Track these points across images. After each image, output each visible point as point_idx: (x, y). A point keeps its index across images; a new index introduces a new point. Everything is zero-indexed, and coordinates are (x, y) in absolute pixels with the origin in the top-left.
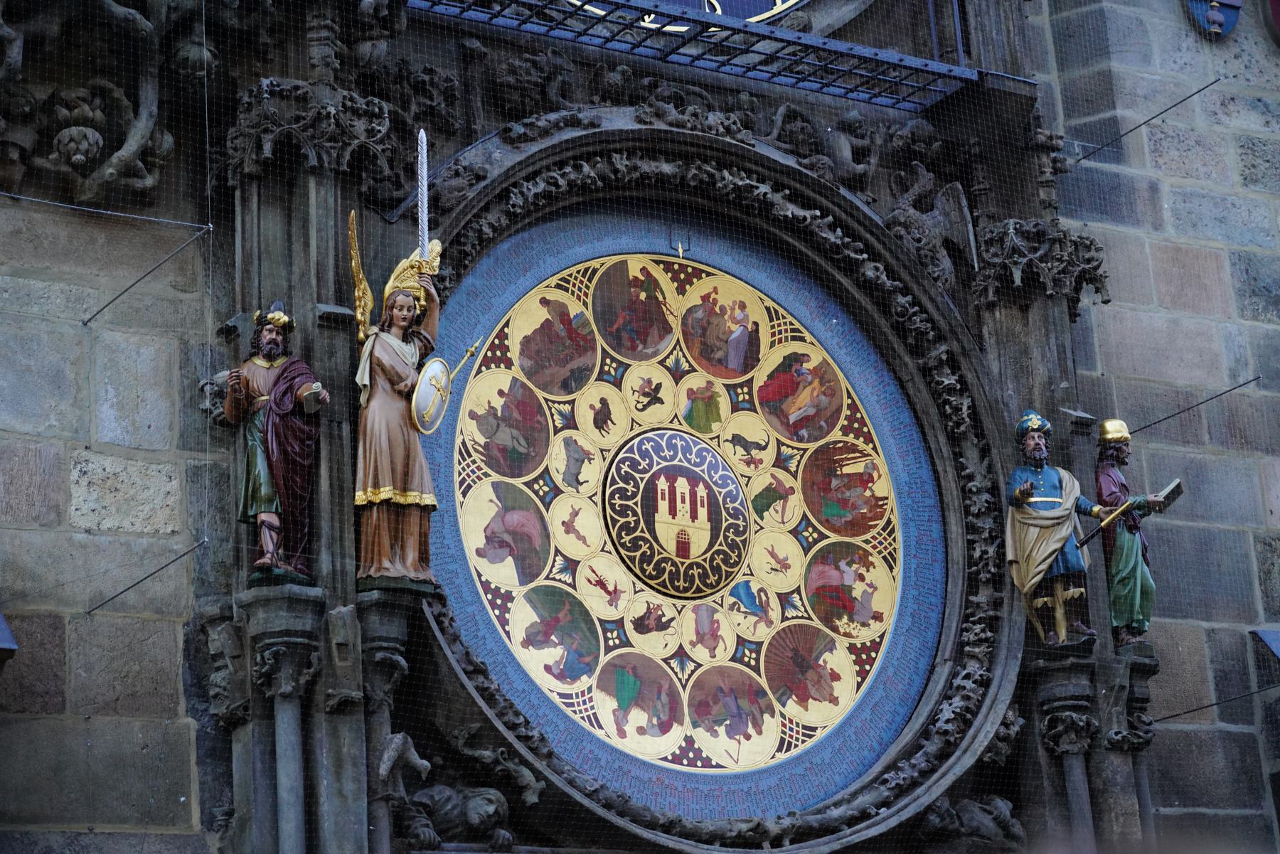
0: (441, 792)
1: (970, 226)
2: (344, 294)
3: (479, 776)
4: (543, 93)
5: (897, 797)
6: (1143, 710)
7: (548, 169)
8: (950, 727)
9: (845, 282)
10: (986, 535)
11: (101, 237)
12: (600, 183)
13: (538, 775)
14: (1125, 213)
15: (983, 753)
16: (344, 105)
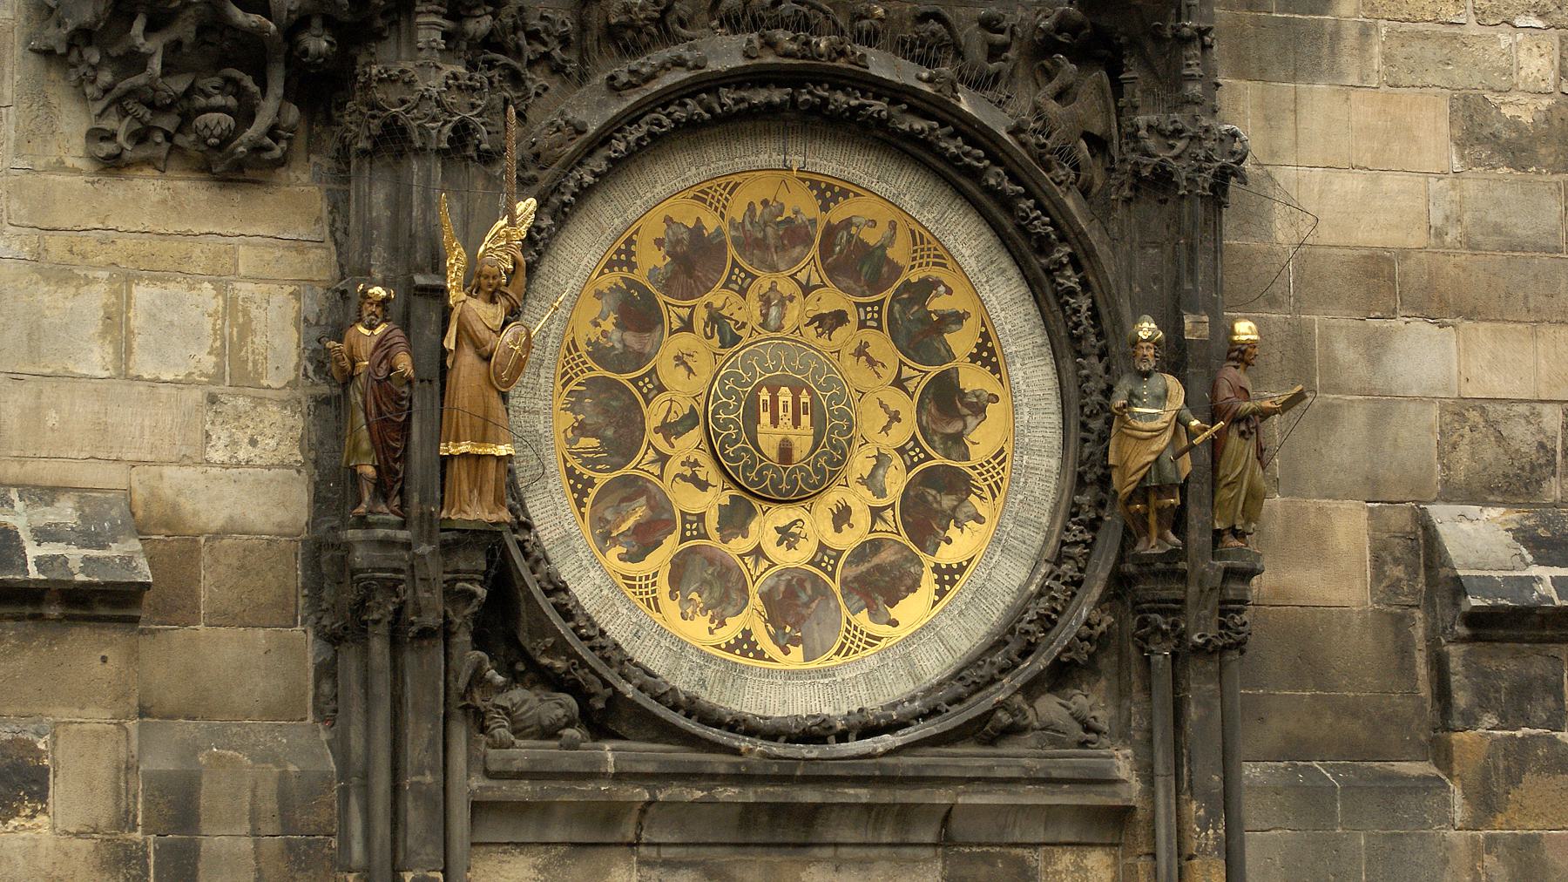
0: (518, 694)
1: (1114, 117)
2: (436, 264)
3: (552, 682)
4: (661, 22)
5: (971, 694)
6: (1239, 612)
7: (653, 111)
8: (1032, 627)
9: (967, 184)
10: (1094, 437)
11: (237, 196)
12: (707, 116)
13: (606, 684)
14: (1324, 67)
15: (1060, 654)
16: (448, 87)
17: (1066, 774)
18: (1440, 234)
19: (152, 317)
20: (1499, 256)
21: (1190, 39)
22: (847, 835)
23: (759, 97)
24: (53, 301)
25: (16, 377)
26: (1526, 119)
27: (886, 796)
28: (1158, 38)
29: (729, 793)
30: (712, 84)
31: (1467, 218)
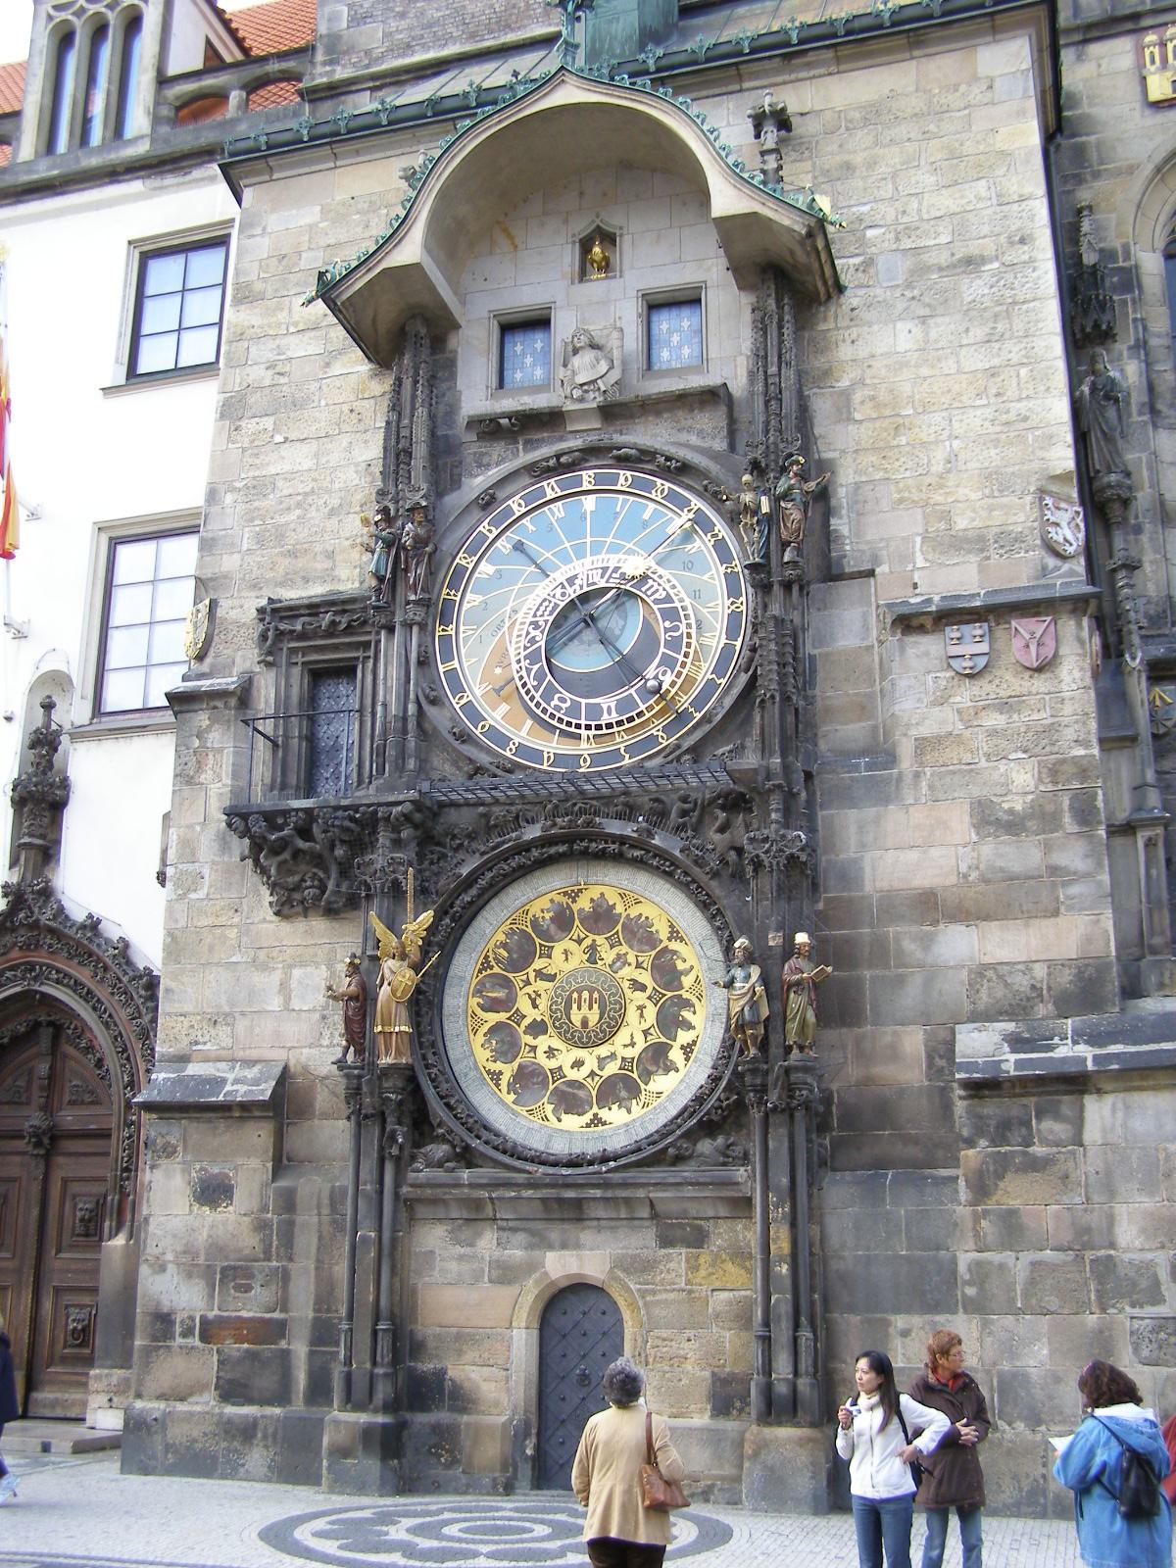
0: (429, 1148)
3: (443, 1139)
17: (708, 1180)
18: (965, 876)
19: (300, 982)
20: (1004, 885)
21: (770, 791)
22: (601, 1214)
23: (553, 850)
24: (258, 979)
25: (243, 1014)
26: (1018, 807)
27: (609, 1194)
28: (759, 793)
29: (529, 1193)
30: (526, 847)
31: (982, 866)
